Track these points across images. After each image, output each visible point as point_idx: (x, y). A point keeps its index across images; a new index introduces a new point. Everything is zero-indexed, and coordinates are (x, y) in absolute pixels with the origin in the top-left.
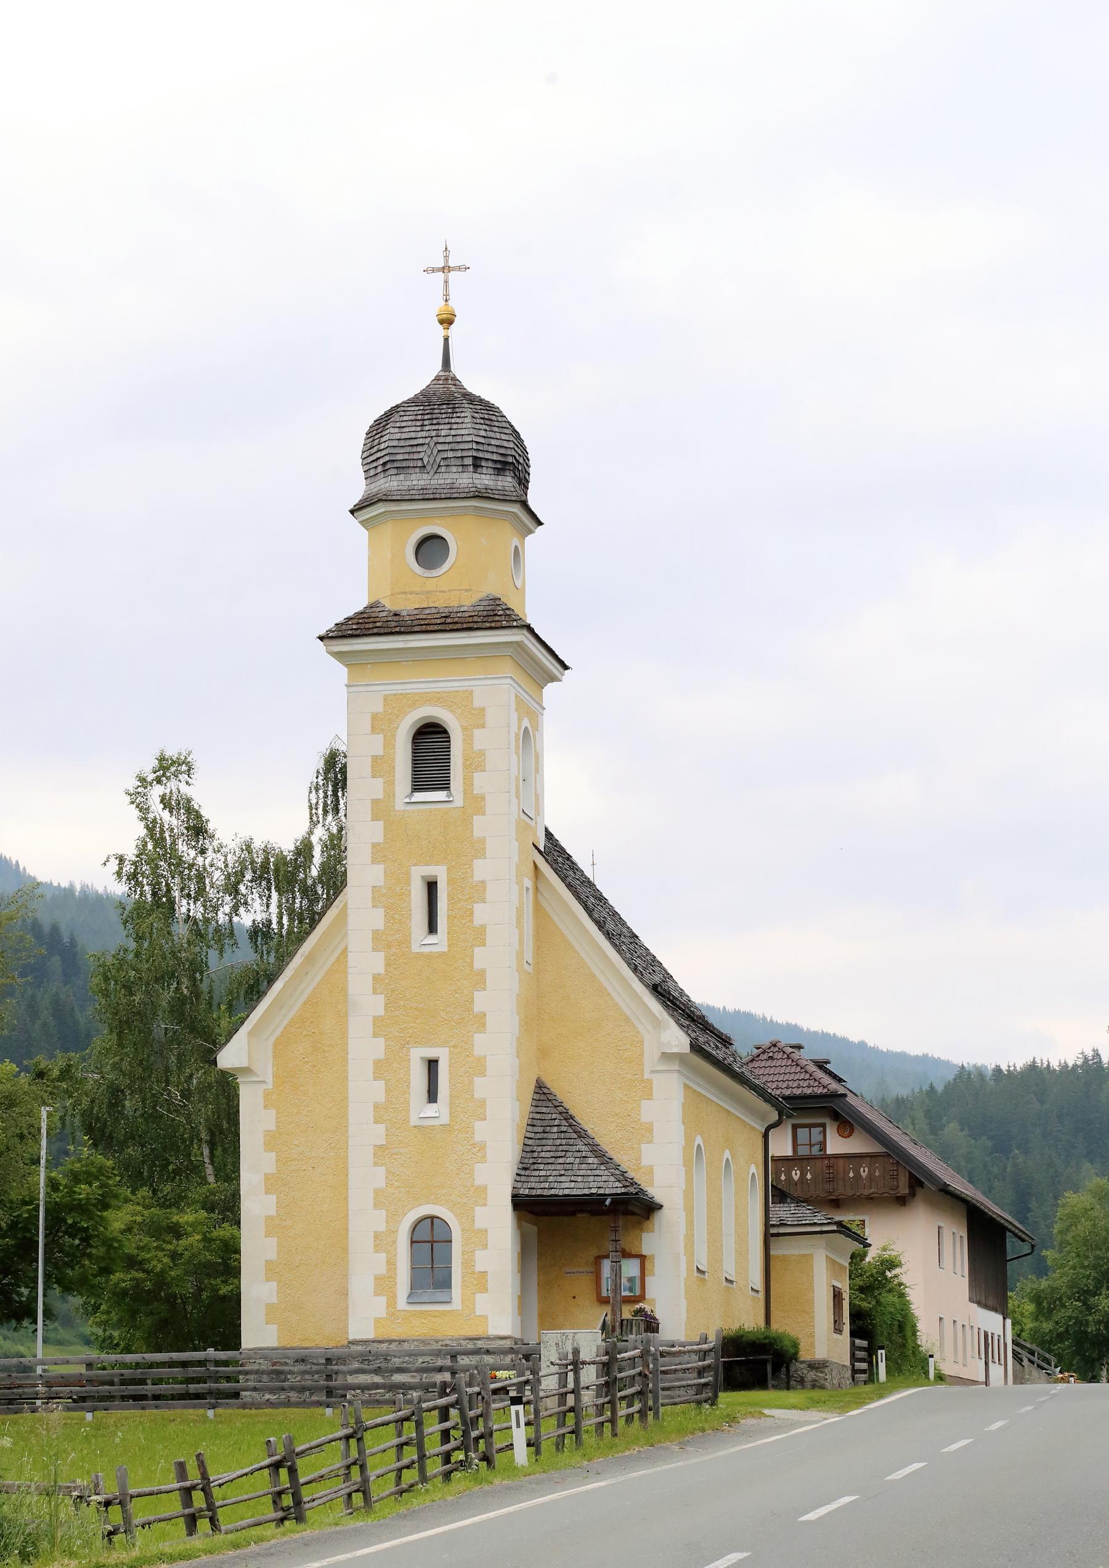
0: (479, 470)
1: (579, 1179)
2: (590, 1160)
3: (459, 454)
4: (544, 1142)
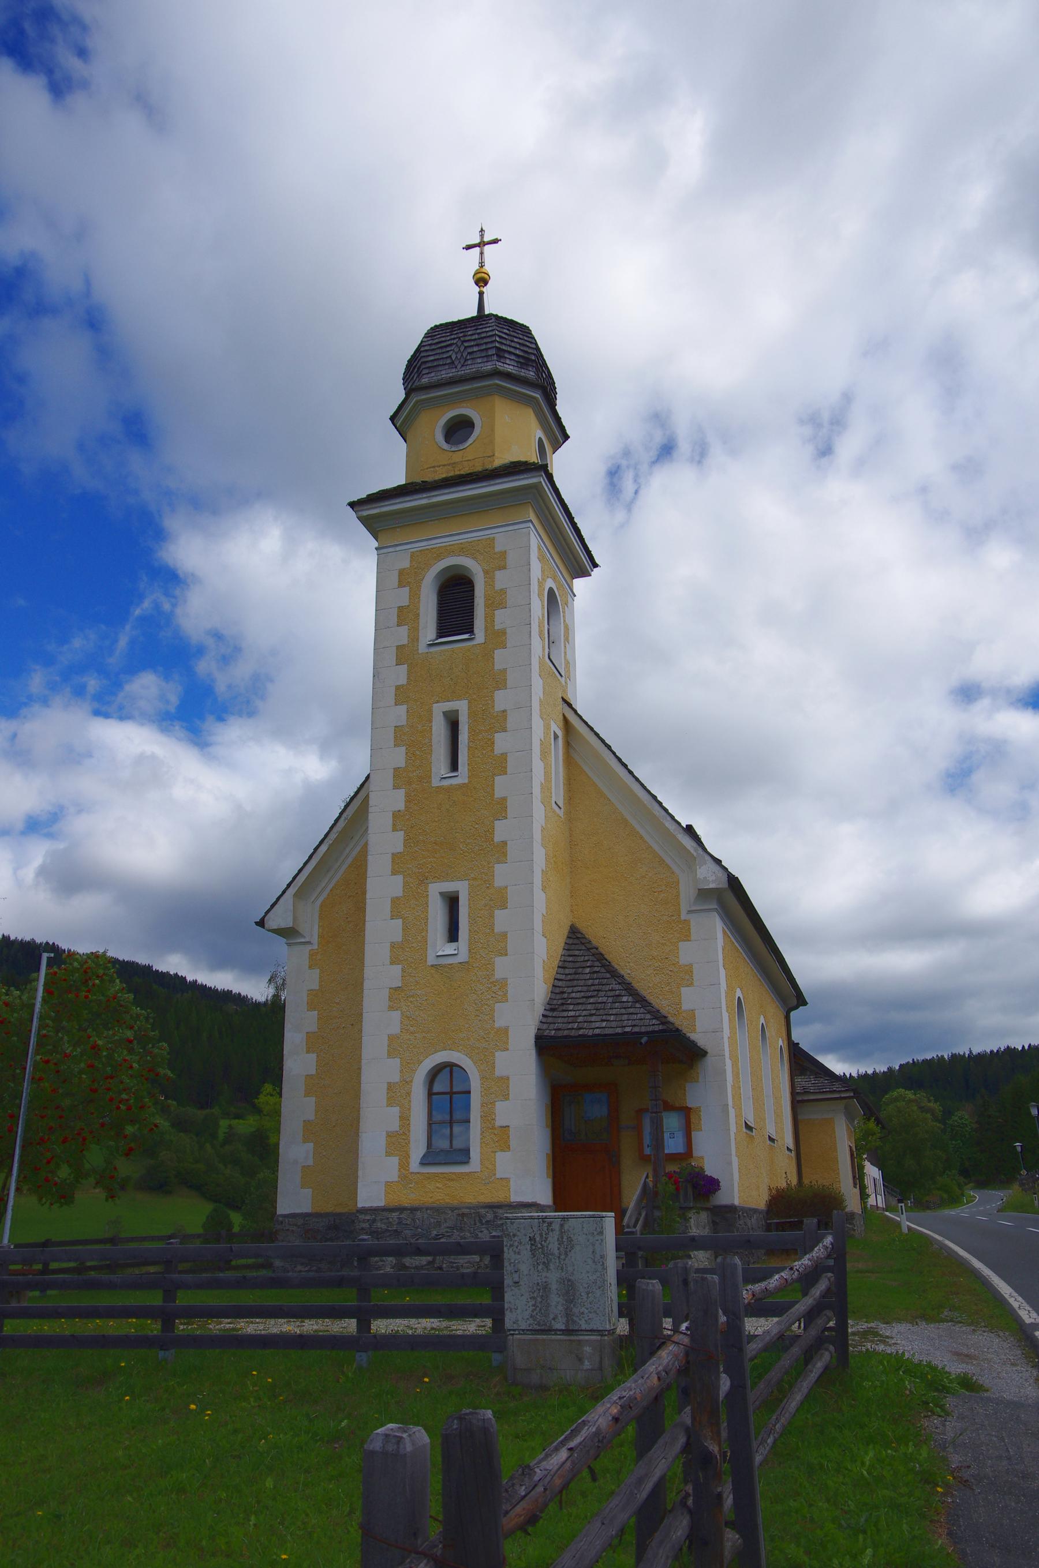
1: (612, 1018)
2: (625, 999)
3: (484, 347)
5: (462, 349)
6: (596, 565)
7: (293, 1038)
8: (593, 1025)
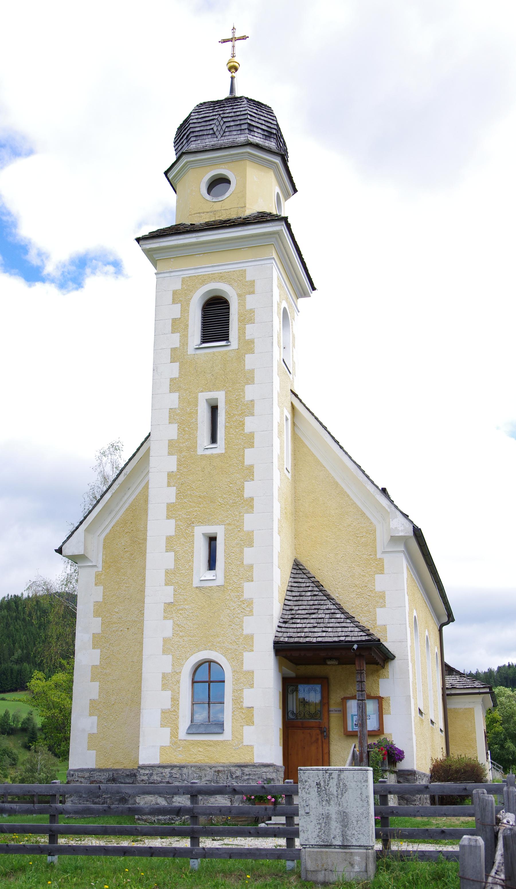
0: (252, 133)
1: (330, 630)
3: (238, 123)
4: (300, 603)
5: (222, 123)
6: (314, 289)
7: (83, 638)
8: (316, 635)
